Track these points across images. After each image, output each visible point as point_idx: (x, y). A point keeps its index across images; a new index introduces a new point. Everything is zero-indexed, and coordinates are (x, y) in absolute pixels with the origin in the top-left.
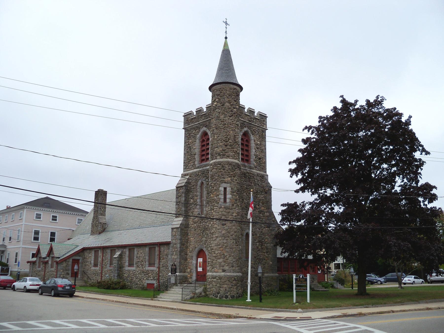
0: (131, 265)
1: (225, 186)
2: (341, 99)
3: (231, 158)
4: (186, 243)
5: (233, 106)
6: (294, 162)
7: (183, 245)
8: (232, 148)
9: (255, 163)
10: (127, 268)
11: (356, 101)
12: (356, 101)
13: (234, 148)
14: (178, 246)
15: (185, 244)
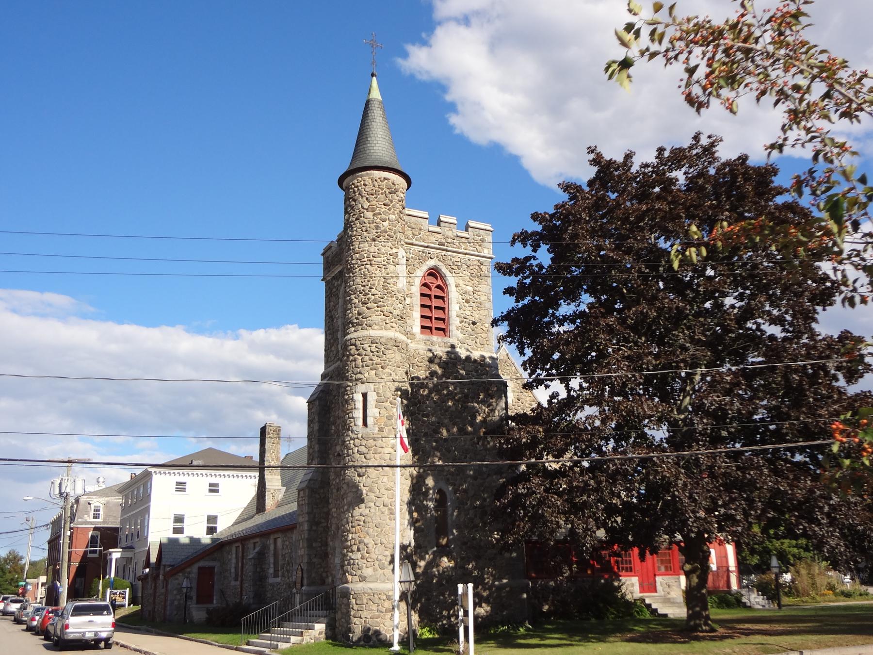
0: (276, 575)
1: (364, 391)
2: (592, 156)
3: (376, 327)
4: (323, 521)
5: (379, 216)
6: (504, 318)
7: (318, 524)
8: (378, 307)
9: (461, 332)
10: (271, 580)
11: (628, 156)
12: (628, 156)
13: (384, 306)
14: (306, 527)
15: (321, 523)
